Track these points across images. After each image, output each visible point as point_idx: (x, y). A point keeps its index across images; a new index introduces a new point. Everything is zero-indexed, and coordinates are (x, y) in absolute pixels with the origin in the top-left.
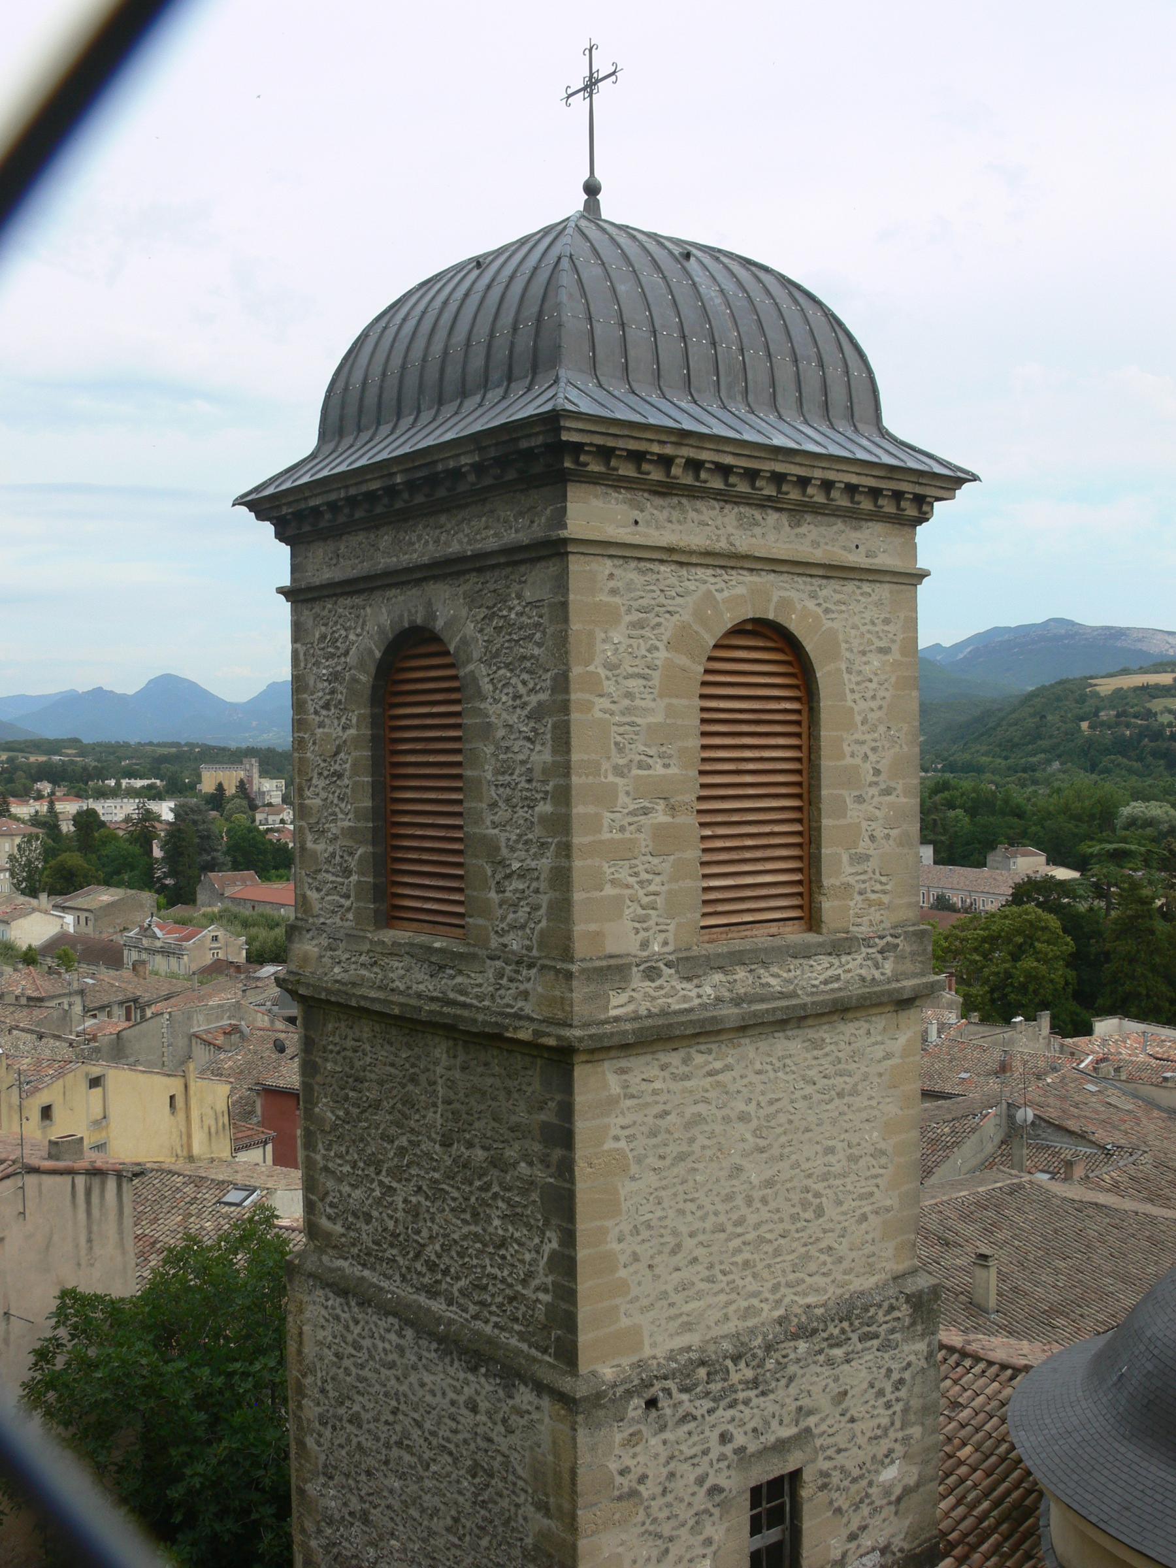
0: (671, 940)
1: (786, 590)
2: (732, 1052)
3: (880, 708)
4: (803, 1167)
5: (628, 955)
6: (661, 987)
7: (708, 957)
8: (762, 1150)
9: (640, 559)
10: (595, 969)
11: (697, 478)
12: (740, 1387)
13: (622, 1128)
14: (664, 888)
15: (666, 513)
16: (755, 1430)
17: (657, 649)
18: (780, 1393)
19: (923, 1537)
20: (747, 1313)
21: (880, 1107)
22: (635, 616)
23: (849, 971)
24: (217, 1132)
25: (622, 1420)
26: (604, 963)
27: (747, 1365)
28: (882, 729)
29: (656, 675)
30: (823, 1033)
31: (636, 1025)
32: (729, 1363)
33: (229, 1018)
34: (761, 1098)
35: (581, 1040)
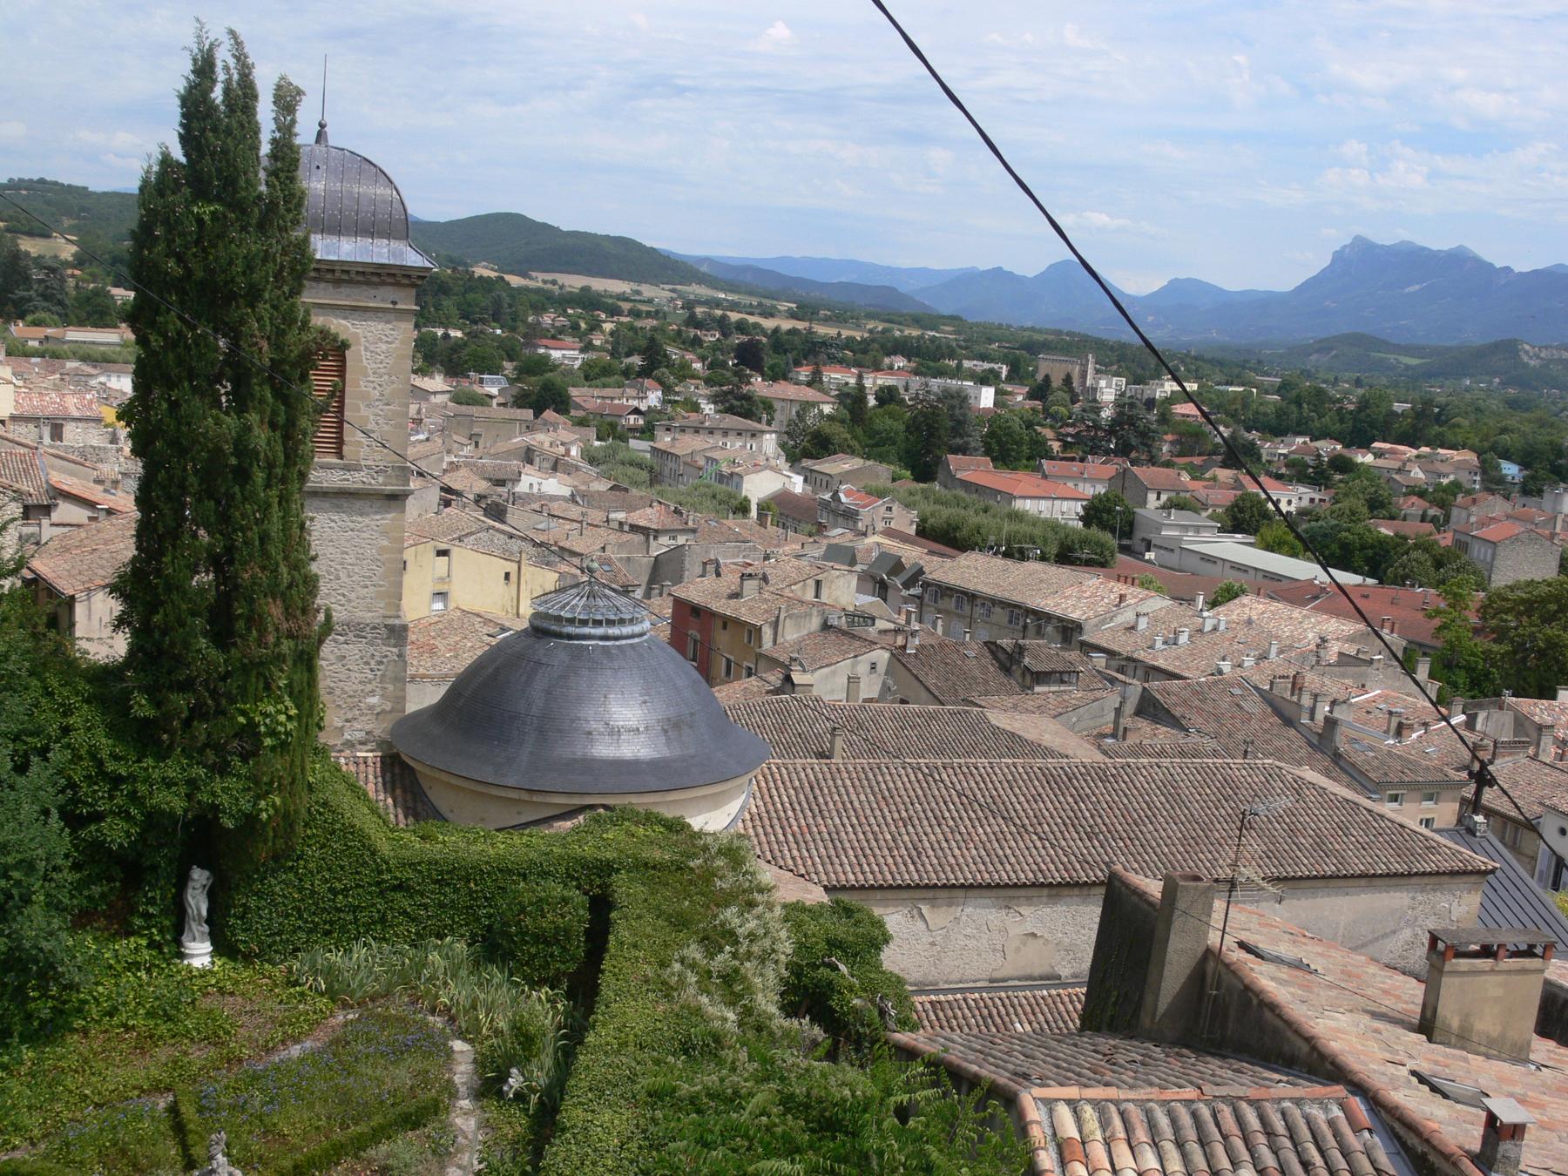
33: (744, 557)
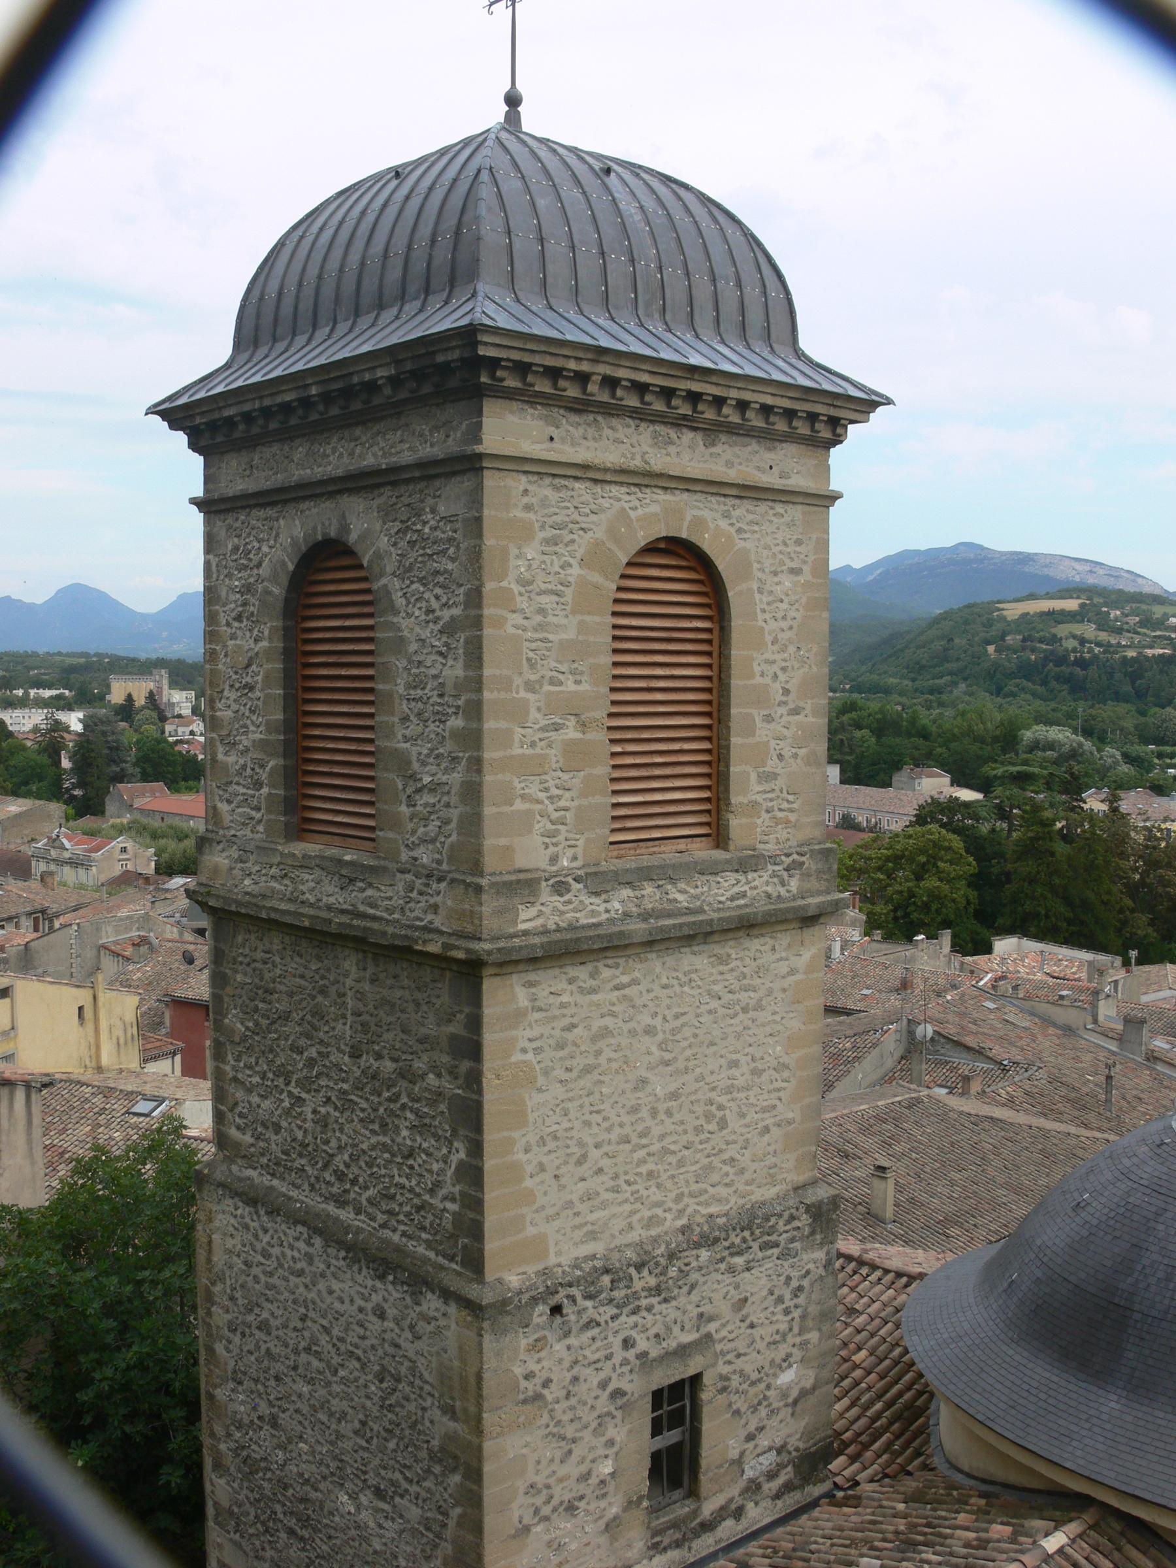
0: (580, 856)
1: (699, 508)
2: (639, 966)
3: (791, 628)
4: (707, 1080)
5: (537, 869)
6: (569, 902)
7: (616, 873)
8: (667, 1064)
9: (554, 475)
10: (505, 883)
11: (613, 396)
12: (643, 1294)
13: (530, 1040)
14: (576, 803)
15: (581, 430)
16: (657, 1336)
17: (570, 566)
18: (682, 1300)
19: (818, 1437)
20: (651, 1222)
21: (784, 1022)
22: (549, 533)
23: (755, 888)
24: (126, 1043)
25: (527, 1326)
26: (514, 877)
27: (650, 1273)
28: (792, 649)
29: (569, 592)
30: (729, 949)
31: (545, 939)
32: (632, 1270)
33: (138, 929)
34: (667, 1012)
35: (489, 953)
